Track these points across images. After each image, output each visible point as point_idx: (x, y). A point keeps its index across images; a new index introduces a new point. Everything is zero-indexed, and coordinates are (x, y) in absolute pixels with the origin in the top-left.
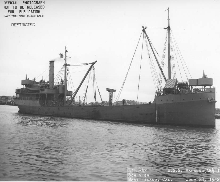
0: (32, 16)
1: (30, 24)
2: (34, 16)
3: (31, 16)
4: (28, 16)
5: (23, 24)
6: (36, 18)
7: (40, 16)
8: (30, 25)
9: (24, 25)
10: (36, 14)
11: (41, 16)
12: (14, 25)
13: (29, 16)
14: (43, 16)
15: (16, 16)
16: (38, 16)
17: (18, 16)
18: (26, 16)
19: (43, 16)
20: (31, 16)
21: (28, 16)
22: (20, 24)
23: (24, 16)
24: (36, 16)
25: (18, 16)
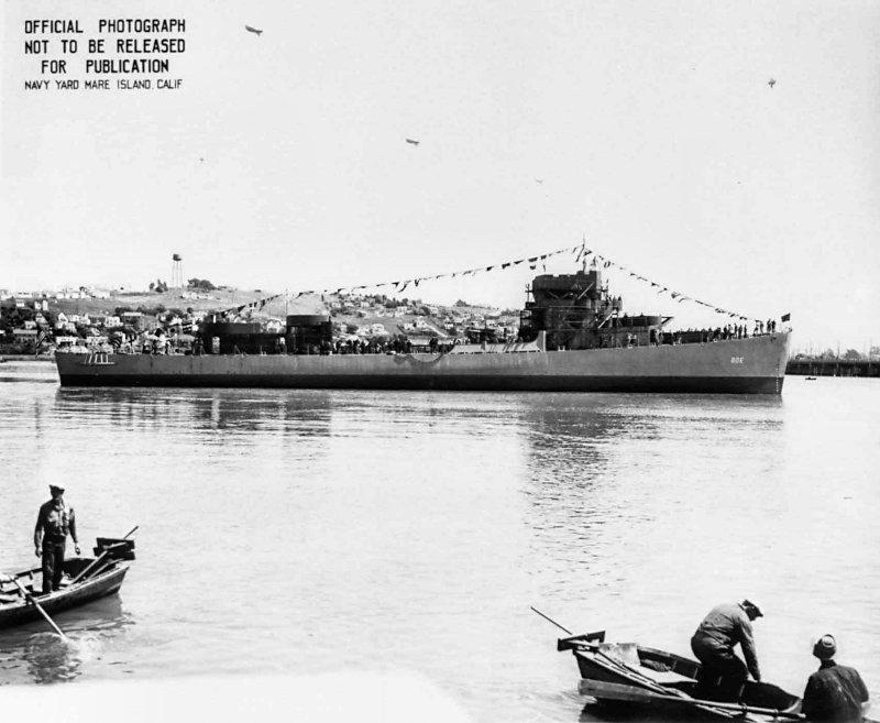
0: (136, 85)
2: (145, 85)
3: (131, 85)
7: (167, 84)
10: (153, 77)
11: (173, 85)
13: (124, 85)
14: (178, 83)
15: (72, 84)
16: (161, 84)
17: (82, 85)
18: (113, 84)
19: (178, 83)
20: (131, 85)
23: (105, 84)
24: (154, 84)
25: (82, 85)
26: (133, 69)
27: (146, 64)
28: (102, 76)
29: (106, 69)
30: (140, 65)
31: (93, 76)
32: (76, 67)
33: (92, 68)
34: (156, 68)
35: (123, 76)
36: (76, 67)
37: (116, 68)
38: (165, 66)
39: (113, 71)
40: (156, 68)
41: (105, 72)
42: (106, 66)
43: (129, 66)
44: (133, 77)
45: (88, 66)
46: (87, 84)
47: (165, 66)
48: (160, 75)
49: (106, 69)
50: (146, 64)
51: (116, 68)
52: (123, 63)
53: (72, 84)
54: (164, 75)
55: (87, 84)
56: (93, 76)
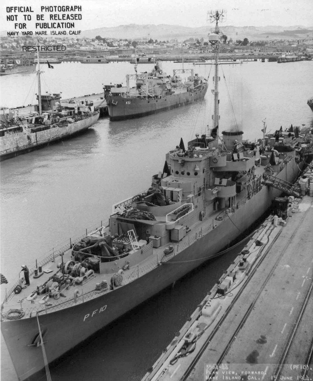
0: (59, 33)
1: (56, 48)
2: (64, 33)
3: (57, 33)
4: (52, 33)
5: (43, 47)
7: (74, 33)
8: (57, 48)
9: (45, 49)
10: (68, 30)
11: (76, 33)
12: (28, 49)
13: (54, 33)
17: (34, 33)
19: (79, 32)
20: (57, 33)
22: (37, 48)
23: (45, 33)
27: (64, 25)
28: (44, 30)
29: (45, 26)
30: (61, 25)
31: (39, 29)
33: (38, 27)
34: (69, 26)
35: (53, 29)
37: (50, 26)
39: (48, 28)
40: (69, 26)
41: (44, 28)
42: (45, 25)
43: (56, 26)
44: (57, 30)
45: (36, 25)
47: (73, 25)
48: (70, 29)
49: (45, 26)
50: (64, 25)
51: (50, 26)
52: (53, 25)
54: (72, 29)
56: (39, 29)
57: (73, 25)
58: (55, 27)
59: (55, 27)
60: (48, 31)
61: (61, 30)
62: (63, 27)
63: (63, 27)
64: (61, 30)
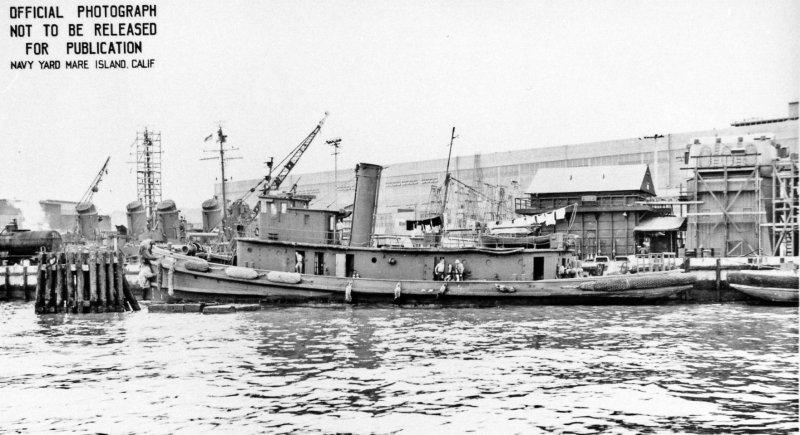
0: (114, 65)
2: (121, 64)
3: (108, 65)
6: (129, 71)
7: (141, 64)
10: (128, 58)
11: (146, 65)
13: (102, 65)
14: (151, 62)
15: (54, 65)
16: (136, 64)
17: (63, 64)
20: (108, 65)
21: (99, 65)
23: (84, 64)
24: (129, 64)
25: (63, 64)
26: (110, 50)
28: (82, 57)
29: (85, 50)
30: (116, 46)
31: (73, 57)
32: (57, 50)
33: (72, 50)
34: (131, 50)
35: (100, 57)
36: (57, 50)
37: (94, 49)
38: (138, 47)
39: (91, 53)
40: (131, 50)
41: (84, 53)
42: (85, 48)
43: (106, 48)
45: (68, 47)
46: (68, 64)
49: (85, 50)
51: (94, 49)
52: (100, 46)
53: (54, 65)
54: (138, 56)
55: (68, 64)
56: (73, 57)
57: (138, 47)
58: (104, 50)
59: (104, 50)
60: (91, 59)
61: (116, 57)
62: (119, 52)
63: (119, 52)
64: (116, 57)
